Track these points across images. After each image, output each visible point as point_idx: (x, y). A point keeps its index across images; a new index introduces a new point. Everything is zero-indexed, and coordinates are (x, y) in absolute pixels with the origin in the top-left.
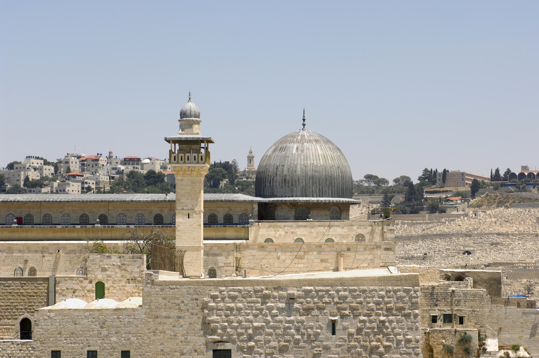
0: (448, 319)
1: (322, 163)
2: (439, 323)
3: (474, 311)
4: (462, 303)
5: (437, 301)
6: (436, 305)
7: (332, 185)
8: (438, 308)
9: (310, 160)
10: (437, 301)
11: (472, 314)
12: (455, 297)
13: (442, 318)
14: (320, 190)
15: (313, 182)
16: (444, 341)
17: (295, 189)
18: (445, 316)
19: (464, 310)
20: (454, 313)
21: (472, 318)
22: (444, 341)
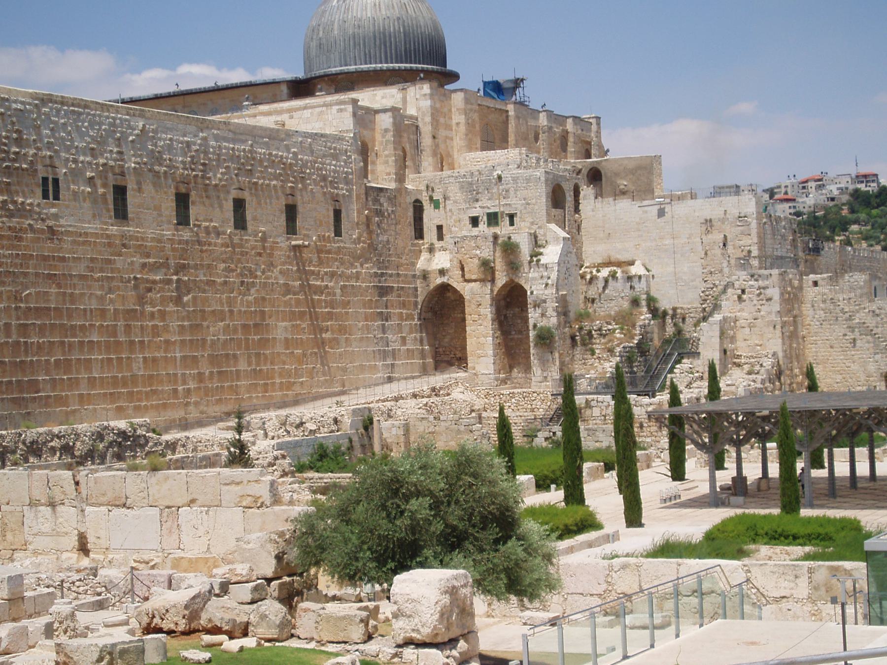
0: (493, 219)
1: (369, 15)
2: (483, 226)
3: (529, 204)
4: (512, 192)
5: (477, 193)
6: (477, 200)
7: (385, 45)
8: (480, 204)
9: (352, 12)
10: (477, 193)
11: (525, 208)
12: (502, 185)
13: (485, 218)
14: (365, 54)
15: (355, 43)
16: (478, 252)
17: (332, 56)
18: (489, 215)
19: (515, 203)
20: (502, 209)
21: (527, 215)
22: (478, 252)
